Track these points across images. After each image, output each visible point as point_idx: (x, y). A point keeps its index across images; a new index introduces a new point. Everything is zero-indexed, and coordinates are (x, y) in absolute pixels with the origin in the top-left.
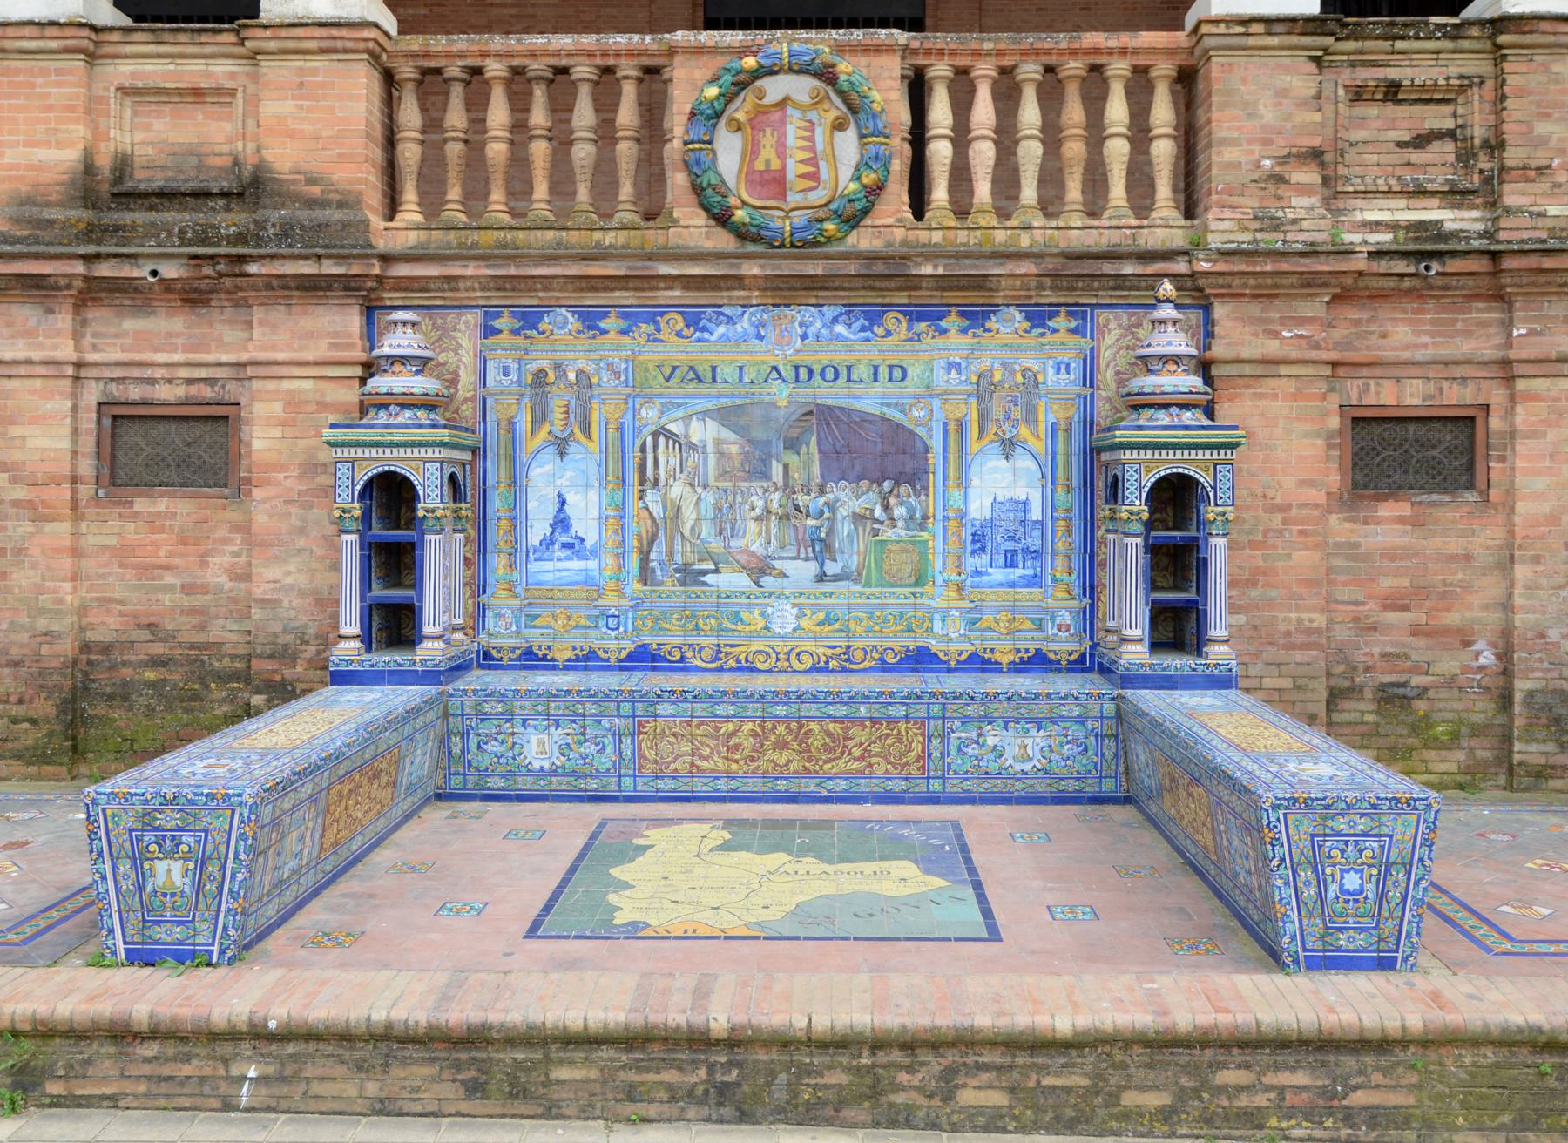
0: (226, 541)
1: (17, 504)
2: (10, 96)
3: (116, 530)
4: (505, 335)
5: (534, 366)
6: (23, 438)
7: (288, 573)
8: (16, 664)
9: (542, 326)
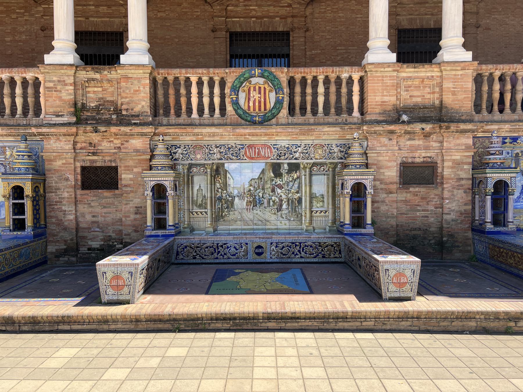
0: (434, 198)
1: (382, 189)
2: (377, 83)
3: (405, 196)
4: (508, 144)
5: (516, 152)
6: (384, 172)
7: (453, 207)
8: (381, 231)
9: (518, 141)
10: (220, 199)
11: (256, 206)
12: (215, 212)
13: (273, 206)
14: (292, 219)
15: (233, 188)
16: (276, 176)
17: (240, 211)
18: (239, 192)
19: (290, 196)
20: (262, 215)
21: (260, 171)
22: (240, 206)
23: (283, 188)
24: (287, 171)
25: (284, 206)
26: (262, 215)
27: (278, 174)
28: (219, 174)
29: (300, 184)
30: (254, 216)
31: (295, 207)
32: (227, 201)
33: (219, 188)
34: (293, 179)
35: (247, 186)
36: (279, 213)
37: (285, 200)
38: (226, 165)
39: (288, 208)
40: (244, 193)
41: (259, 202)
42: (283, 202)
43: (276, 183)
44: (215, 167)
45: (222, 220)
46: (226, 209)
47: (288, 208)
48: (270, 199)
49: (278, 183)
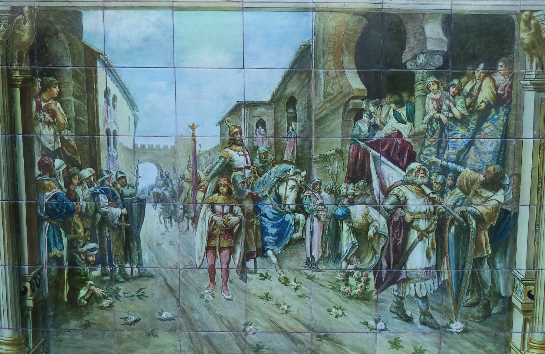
10: (61, 212)
11: (262, 252)
12: (37, 282)
13: (358, 254)
14: (457, 326)
15: (134, 151)
16: (376, 92)
17: (174, 282)
18: (165, 178)
19: (449, 200)
20: (296, 305)
21: (287, 57)
22: (171, 255)
23: (412, 158)
24: (438, 61)
25: (418, 259)
26: (296, 305)
27: (389, 80)
28: (52, 73)
29: (509, 134)
30: (249, 309)
31: (478, 262)
32: (99, 223)
33: (57, 154)
34: (471, 107)
35: (210, 140)
36: (389, 295)
37: (423, 225)
38: (91, 23)
39: (438, 266)
40: (197, 183)
41: (280, 236)
42: (414, 235)
43: (374, 127)
44: (26, 34)
45: (74, 324)
46: (94, 265)
47: (438, 266)
48: (337, 220)
49: (387, 130)
